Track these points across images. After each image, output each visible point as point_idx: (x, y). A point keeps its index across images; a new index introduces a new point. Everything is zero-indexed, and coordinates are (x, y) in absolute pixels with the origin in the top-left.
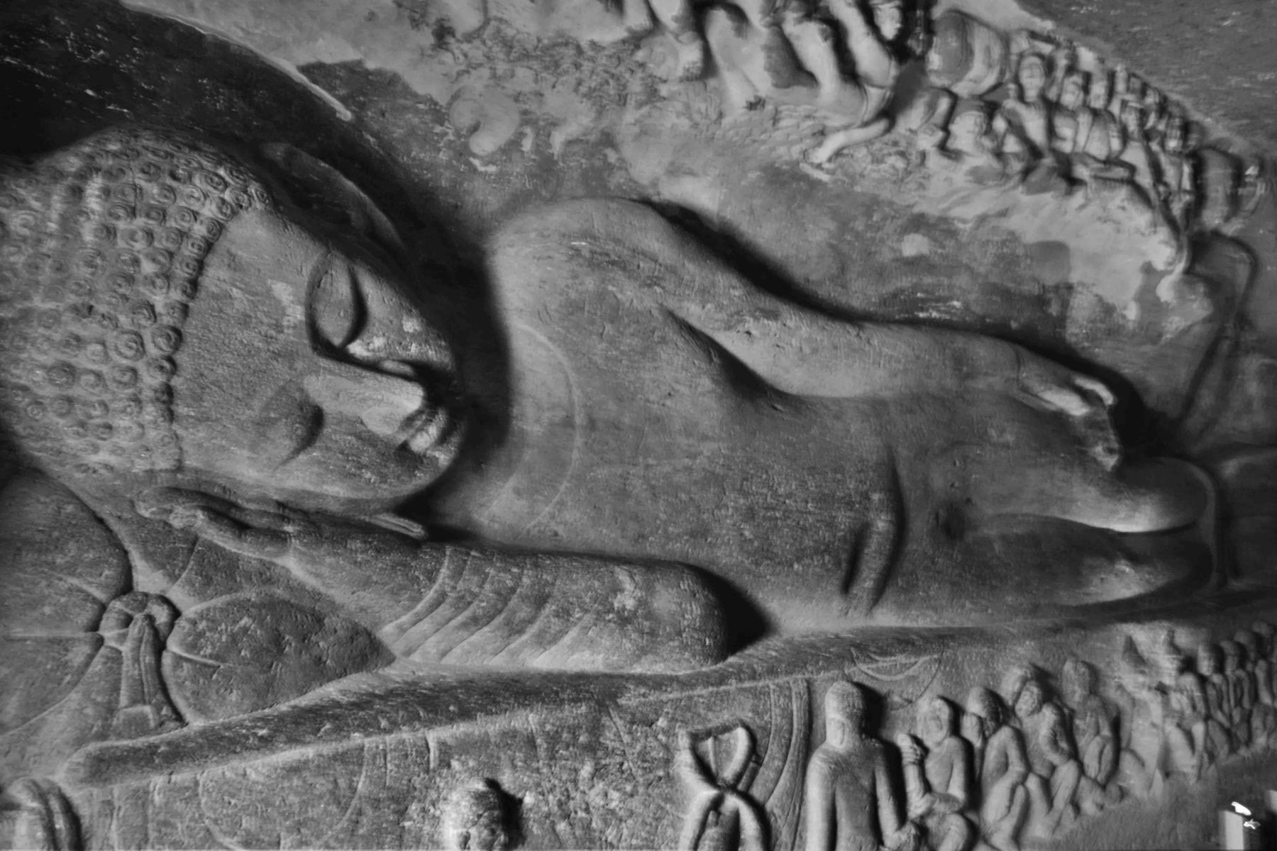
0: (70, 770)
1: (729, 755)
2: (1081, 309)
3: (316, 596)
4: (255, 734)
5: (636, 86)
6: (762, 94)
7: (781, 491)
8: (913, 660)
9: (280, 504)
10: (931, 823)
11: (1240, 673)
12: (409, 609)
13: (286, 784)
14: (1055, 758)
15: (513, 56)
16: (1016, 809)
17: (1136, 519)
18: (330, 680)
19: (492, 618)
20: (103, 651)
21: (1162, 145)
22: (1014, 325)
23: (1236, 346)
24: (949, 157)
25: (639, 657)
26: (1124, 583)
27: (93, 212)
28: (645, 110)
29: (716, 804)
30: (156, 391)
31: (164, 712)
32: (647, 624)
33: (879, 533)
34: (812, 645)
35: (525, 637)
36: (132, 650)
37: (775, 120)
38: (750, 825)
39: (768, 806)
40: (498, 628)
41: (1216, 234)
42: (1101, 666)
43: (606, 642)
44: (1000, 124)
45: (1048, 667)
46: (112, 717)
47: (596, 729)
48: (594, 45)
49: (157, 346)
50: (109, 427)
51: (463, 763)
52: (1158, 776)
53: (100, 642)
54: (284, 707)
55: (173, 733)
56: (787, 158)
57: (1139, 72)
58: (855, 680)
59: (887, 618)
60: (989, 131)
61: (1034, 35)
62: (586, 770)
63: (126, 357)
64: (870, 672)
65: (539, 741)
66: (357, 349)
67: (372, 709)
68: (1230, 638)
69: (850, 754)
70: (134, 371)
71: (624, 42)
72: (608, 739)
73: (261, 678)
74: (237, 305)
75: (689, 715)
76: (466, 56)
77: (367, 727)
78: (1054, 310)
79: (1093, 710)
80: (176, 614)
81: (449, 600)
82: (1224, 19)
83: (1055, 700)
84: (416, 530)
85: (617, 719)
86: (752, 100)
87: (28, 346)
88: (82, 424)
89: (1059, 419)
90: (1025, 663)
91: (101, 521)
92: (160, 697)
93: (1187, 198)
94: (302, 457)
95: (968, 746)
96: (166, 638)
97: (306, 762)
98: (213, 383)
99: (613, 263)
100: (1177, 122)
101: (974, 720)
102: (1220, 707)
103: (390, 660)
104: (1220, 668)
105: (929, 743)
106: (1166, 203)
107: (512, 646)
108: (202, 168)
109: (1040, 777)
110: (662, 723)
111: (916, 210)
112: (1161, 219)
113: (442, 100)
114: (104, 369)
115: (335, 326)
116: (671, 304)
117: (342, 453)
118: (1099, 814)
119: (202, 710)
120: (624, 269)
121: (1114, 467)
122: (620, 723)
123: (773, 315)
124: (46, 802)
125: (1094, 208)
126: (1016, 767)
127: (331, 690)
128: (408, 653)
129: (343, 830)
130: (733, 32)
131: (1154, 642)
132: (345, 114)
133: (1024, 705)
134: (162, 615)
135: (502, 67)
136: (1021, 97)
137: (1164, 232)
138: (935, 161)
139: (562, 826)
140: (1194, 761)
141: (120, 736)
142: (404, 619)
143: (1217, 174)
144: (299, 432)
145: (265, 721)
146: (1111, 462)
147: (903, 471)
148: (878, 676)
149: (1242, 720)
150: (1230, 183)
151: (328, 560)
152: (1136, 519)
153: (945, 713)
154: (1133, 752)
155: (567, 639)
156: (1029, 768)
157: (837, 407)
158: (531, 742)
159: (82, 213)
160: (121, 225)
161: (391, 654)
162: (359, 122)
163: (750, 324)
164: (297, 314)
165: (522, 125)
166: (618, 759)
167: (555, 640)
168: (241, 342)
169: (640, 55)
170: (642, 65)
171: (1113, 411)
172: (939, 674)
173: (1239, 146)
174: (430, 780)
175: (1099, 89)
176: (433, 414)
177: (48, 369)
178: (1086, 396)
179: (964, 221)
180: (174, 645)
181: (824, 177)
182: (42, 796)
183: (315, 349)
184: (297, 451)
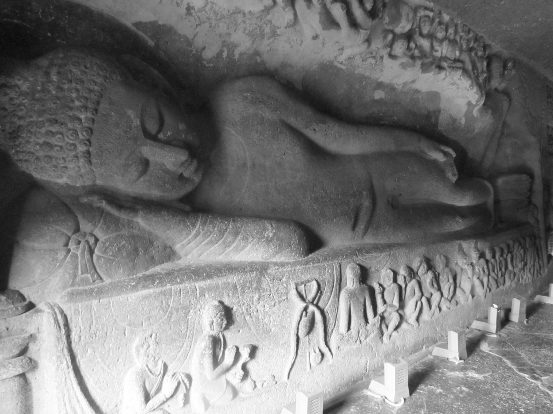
0: (62, 298)
1: (310, 291)
2: (443, 119)
3: (150, 233)
4: (131, 285)
5: (267, 30)
6: (318, 33)
7: (328, 191)
10: (386, 315)
11: (501, 258)
12: (186, 238)
13: (143, 303)
14: (432, 290)
15: (218, 17)
16: (418, 309)
17: (464, 201)
18: (157, 265)
19: (218, 241)
20: (70, 254)
21: (476, 54)
22: (418, 127)
23: (503, 133)
24: (393, 59)
25: (275, 255)
26: (458, 225)
27: (55, 82)
28: (272, 40)
29: (306, 309)
30: (84, 153)
31: (96, 276)
32: (278, 242)
34: (341, 250)
35: (231, 248)
36: (82, 253)
37: (323, 44)
38: (318, 317)
39: (325, 310)
40: (221, 245)
41: (496, 89)
42: (450, 256)
43: (262, 249)
44: (412, 45)
45: (430, 257)
46: (76, 278)
47: (259, 282)
48: (250, 12)
49: (83, 136)
50: (66, 167)
51: (209, 295)
52: (470, 296)
53: (69, 251)
54: (140, 275)
55: (98, 284)
56: (328, 59)
57: (468, 24)
59: (369, 240)
60: (409, 49)
61: (426, 8)
62: (256, 296)
63: (70, 139)
65: (238, 287)
66: (161, 136)
67: (174, 275)
68: (498, 246)
69: (356, 290)
70: (74, 145)
71: (263, 11)
72: (264, 285)
73: (131, 264)
74: (114, 118)
75: (295, 277)
76: (199, 18)
77: (172, 282)
78: (433, 120)
80: (97, 240)
81: (201, 234)
83: (433, 269)
84: (188, 208)
85: (267, 278)
86: (315, 35)
87: (33, 137)
88: (56, 167)
89: (435, 162)
90: (422, 256)
91: (66, 205)
92: (93, 270)
93: (485, 75)
94: (142, 179)
95: (400, 287)
96: (94, 249)
97: (151, 294)
98: (106, 150)
99: (261, 102)
100: (482, 44)
101: (403, 277)
102: (494, 271)
103: (180, 258)
104: (494, 257)
105: (385, 286)
106: (477, 77)
107: (226, 252)
108: (96, 63)
109: (427, 298)
110: (284, 279)
111: (379, 80)
112: (475, 84)
113: (190, 37)
114: (64, 144)
115: (152, 127)
116: (284, 118)
117: (158, 177)
118: (448, 311)
119: (110, 276)
120: (265, 104)
121: (456, 182)
122: (268, 280)
123: (324, 122)
124: (54, 310)
125: (448, 79)
126: (418, 294)
127: (158, 269)
128: (186, 255)
129: (166, 319)
130: (306, 7)
131: (470, 247)
132: (151, 43)
134: (92, 241)
135: (214, 22)
136: (421, 34)
137: (475, 89)
138: (387, 61)
139: (247, 318)
140: (484, 291)
141: (79, 286)
142: (184, 242)
143: (496, 66)
144: (141, 169)
145: (133, 279)
146: (454, 179)
147: (375, 183)
149: (502, 276)
150: (502, 69)
151: (154, 219)
152: (464, 201)
153: (392, 274)
155: (247, 248)
156: (422, 295)
157: (350, 158)
158: (235, 287)
159: (50, 82)
160: (66, 87)
161: (180, 256)
162: (157, 46)
163: (315, 126)
164: (137, 122)
165: (222, 47)
166: (269, 293)
167: (242, 249)
168: (116, 134)
169: (269, 17)
170: (270, 21)
171: (456, 160)
173: (506, 53)
174: (198, 301)
175: (451, 31)
176: (192, 162)
177: (41, 145)
178: (445, 154)
180: (96, 251)
181: (344, 67)
182: (52, 308)
183: (145, 136)
184: (139, 177)
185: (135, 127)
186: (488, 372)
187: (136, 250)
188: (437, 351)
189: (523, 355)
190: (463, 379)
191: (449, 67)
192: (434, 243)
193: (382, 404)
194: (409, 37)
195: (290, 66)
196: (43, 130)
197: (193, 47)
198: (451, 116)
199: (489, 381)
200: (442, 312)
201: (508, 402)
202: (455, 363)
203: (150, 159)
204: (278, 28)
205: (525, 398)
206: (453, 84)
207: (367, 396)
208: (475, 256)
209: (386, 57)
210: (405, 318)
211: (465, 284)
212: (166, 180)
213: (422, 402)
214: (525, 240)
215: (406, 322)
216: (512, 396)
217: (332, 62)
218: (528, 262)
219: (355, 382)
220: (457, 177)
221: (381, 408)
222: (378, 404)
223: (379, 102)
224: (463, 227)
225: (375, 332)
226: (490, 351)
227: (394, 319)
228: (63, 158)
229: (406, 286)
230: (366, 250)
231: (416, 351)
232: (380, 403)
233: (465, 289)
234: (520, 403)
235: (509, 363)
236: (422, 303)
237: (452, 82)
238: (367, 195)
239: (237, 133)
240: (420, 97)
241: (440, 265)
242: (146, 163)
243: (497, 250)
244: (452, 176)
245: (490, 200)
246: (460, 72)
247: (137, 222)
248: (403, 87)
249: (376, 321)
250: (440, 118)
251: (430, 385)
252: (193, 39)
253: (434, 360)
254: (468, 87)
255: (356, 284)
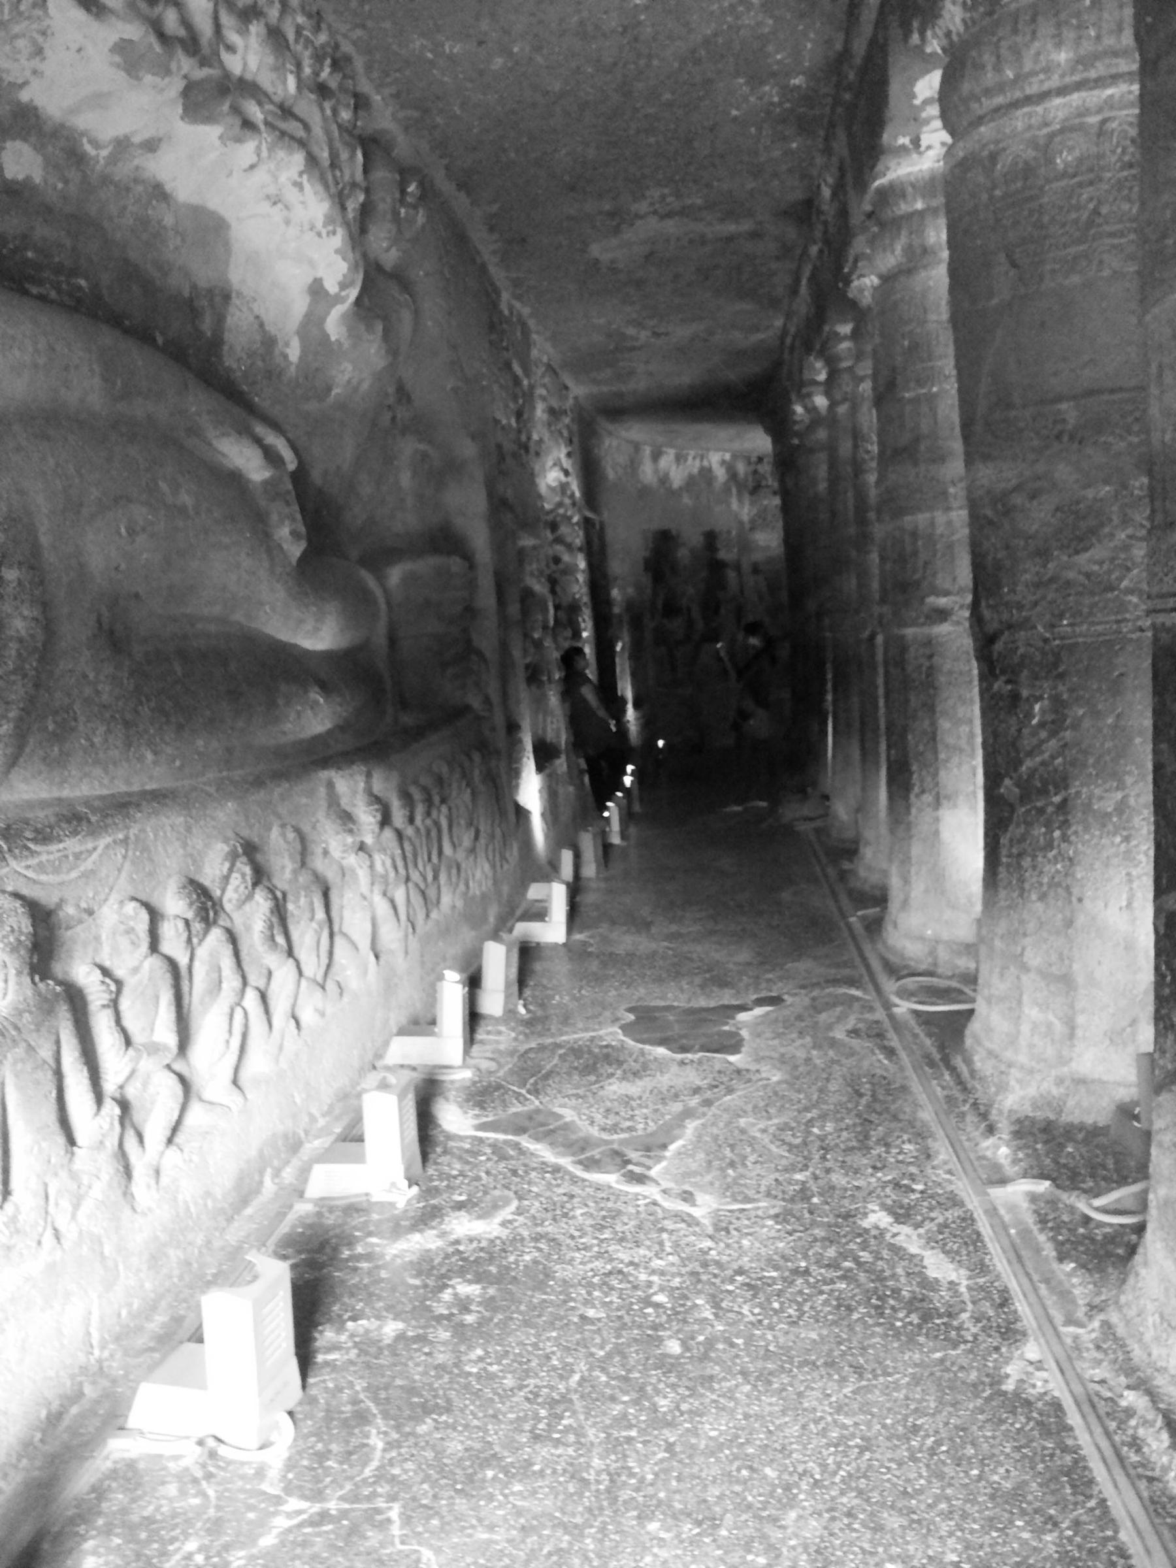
8: (90, 846)
10: (131, 1093)
11: (428, 822)
14: (273, 960)
17: (318, 634)
26: (315, 717)
33: (21, 640)
42: (306, 828)
52: (372, 958)
58: (10, 889)
64: (30, 874)
68: (415, 782)
78: (207, 325)
79: (306, 888)
95: (173, 965)
101: (181, 925)
102: (416, 865)
104: (411, 820)
105: (120, 973)
109: (258, 989)
111: (24, 96)
125: (261, 176)
126: (231, 982)
133: (230, 897)
140: (401, 934)
146: (295, 550)
148: (43, 878)
152: (318, 634)
154: (345, 935)
156: (245, 982)
172: (127, 865)
186: (507, 1202)
188: (332, 1182)
189: (569, 1115)
190: (447, 1256)
192: (258, 783)
193: (209, 1476)
198: (262, 325)
199: (525, 1233)
200: (303, 1032)
201: (612, 1288)
202: (392, 1205)
205: (649, 1254)
206: (276, 200)
207: (131, 1465)
208: (372, 820)
210: (194, 1088)
211: (354, 921)
213: (355, 1402)
214: (471, 760)
215: (201, 1100)
216: (611, 1260)
218: (482, 828)
219: (54, 1418)
221: (211, 1493)
222: (195, 1481)
224: (328, 725)
225: (105, 1177)
226: (482, 1127)
227: (158, 1101)
229: (192, 959)
230: (37, 831)
231: (245, 1201)
232: (199, 1474)
233: (355, 937)
234: (643, 1277)
235: (544, 1152)
236: (246, 1013)
237: (272, 190)
238: (20, 583)
240: (169, 220)
241: (283, 868)
243: (417, 795)
244: (290, 540)
245: (380, 639)
246: (298, 159)
248: (113, 160)
249: (106, 1126)
250: (229, 320)
251: (354, 1319)
253: (319, 1214)
254: (319, 225)
255: (19, 984)
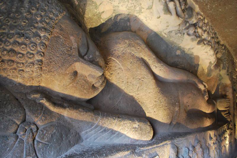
9: (62, 98)
12: (91, 127)
21: (214, 40)
27: (26, 8)
32: (141, 132)
35: (115, 135)
40: (109, 133)
56: (160, 31)
82: (231, 18)
92: (34, 154)
94: (71, 85)
107: (111, 137)
111: (179, 45)
121: (207, 100)
128: (86, 139)
137: (214, 57)
138: (186, 36)
146: (207, 99)
162: (79, 5)
175: (208, 27)
179: (186, 49)
181: (166, 36)
185: (74, 48)
187: (61, 136)
191: (207, 44)
194: (195, 25)
195: (142, 31)
196: (12, 41)
197: (98, 10)
198: (203, 68)
203: (78, 72)
204: (143, 9)
206: (207, 52)
209: (186, 33)
212: (85, 87)
217: (161, 32)
220: (208, 98)
223: (178, 56)
228: (23, 63)
237: (206, 51)
239: (120, 62)
242: (75, 73)
246: (210, 47)
247: (63, 116)
248: (188, 51)
250: (199, 68)
252: (99, 5)
